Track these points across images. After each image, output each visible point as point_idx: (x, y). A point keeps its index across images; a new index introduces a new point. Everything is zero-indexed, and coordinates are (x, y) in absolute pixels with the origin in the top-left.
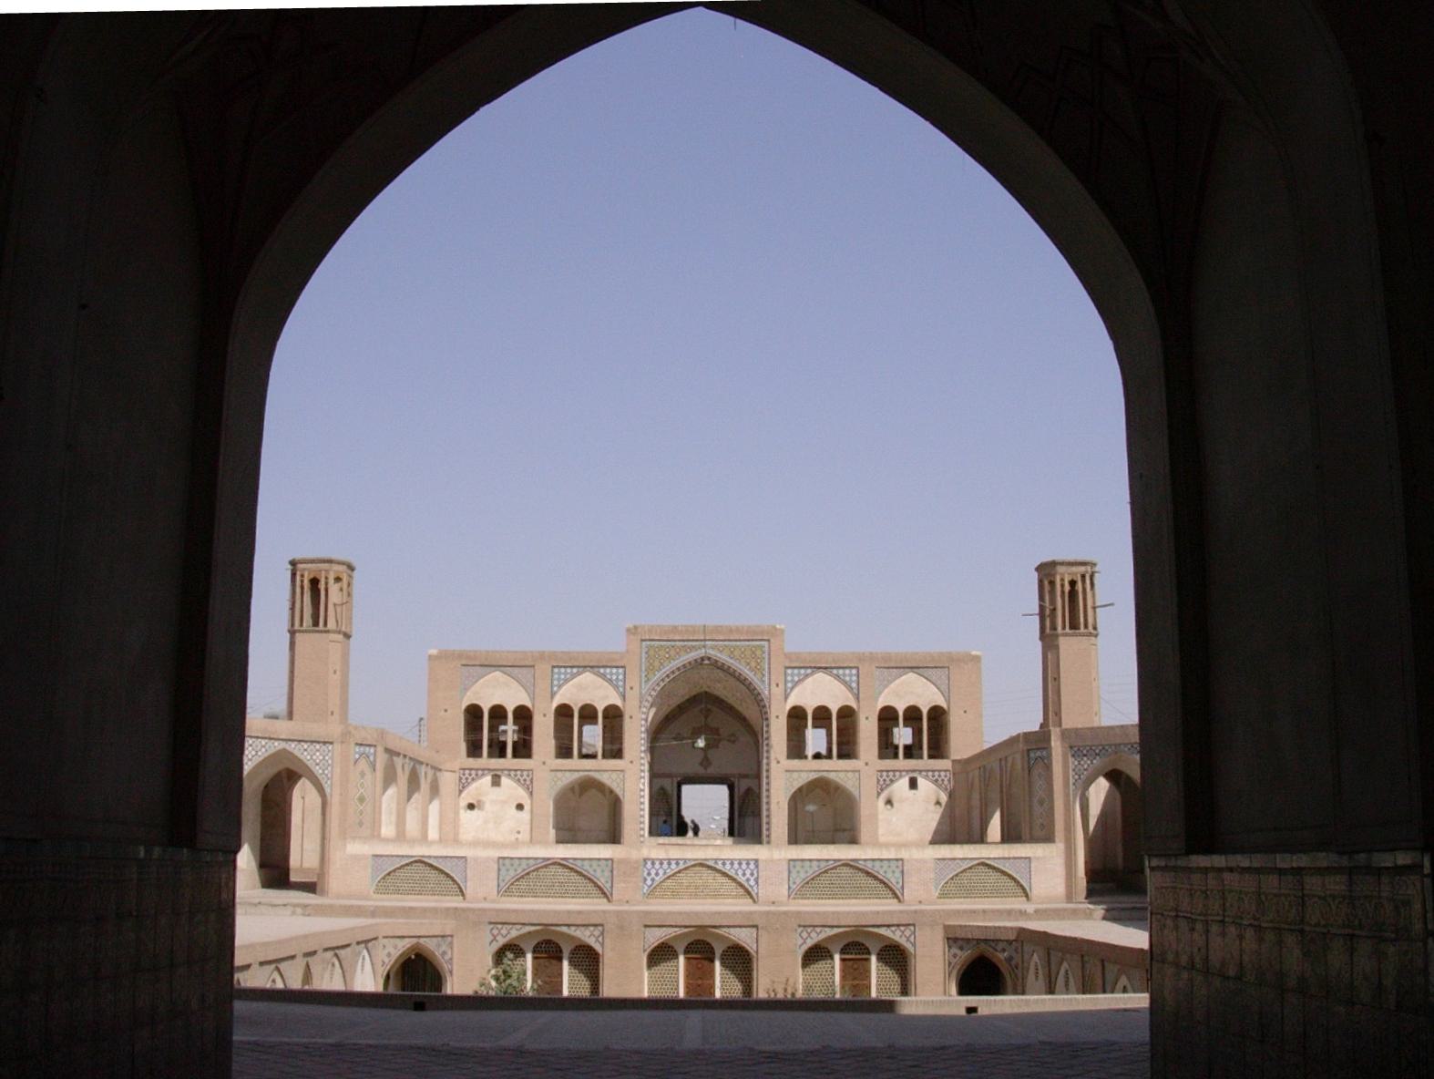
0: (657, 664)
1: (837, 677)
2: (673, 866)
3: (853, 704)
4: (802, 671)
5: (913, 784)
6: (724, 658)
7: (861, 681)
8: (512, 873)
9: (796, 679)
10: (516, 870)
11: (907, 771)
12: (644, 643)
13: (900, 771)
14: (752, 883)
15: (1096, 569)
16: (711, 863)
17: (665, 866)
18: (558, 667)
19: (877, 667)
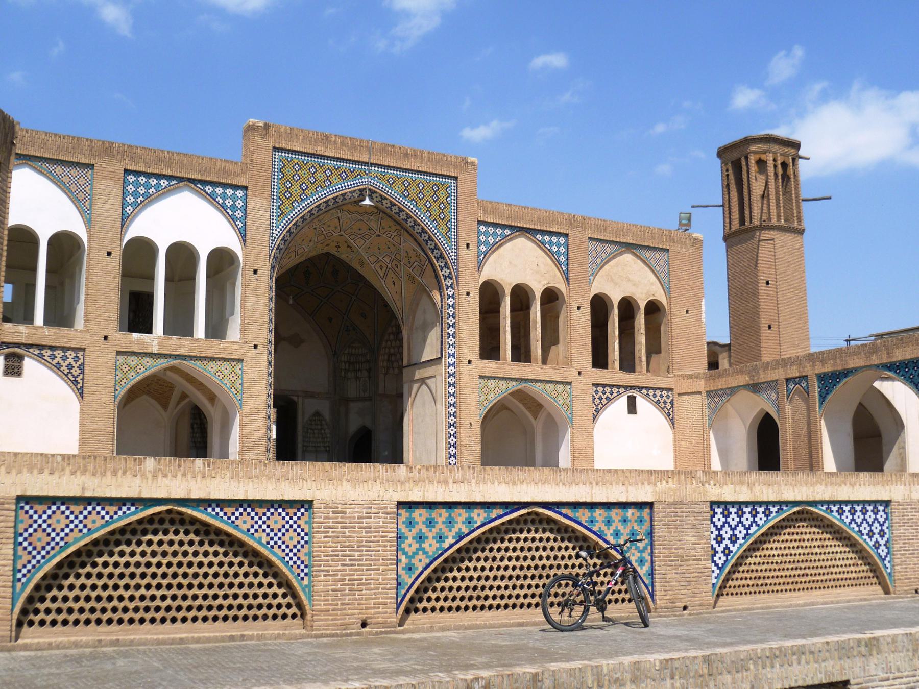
0: (296, 190)
1: (541, 245)
2: (761, 519)
3: (561, 286)
4: (499, 231)
5: (632, 408)
6: (395, 194)
7: (571, 254)
8: (431, 546)
9: (491, 240)
10: (440, 538)
11: (627, 388)
12: (278, 154)
13: (619, 387)
14: (883, 551)
15: (801, 153)
16: (820, 511)
17: (747, 519)
18: (138, 173)
19: (590, 238)
